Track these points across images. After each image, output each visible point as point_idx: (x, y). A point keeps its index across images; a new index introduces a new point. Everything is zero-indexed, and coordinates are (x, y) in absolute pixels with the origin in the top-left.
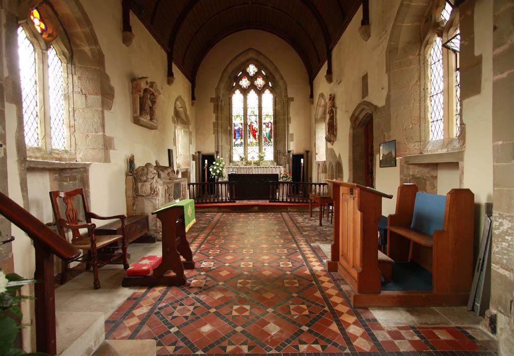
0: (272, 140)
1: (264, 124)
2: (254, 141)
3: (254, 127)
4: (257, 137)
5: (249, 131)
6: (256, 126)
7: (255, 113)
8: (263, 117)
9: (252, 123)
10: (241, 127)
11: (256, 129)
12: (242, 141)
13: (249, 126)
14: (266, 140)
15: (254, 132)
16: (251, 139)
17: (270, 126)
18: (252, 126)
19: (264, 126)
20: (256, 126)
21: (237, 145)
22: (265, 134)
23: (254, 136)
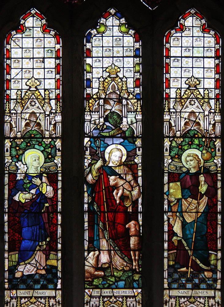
0: (216, 257)
1: (173, 177)
2: (118, 261)
3: (117, 195)
4: (133, 241)
5: (91, 212)
6: (127, 188)
7: (124, 125)
8: (167, 143)
9: (106, 171)
10: (47, 190)
11: (128, 204)
12: (56, 261)
13: (93, 187)
14: (181, 258)
15: (113, 217)
16: (100, 256)
17: (203, 188)
18: (111, 189)
19: (174, 190)
20: (127, 188)
21: (28, 282)
22: (177, 228)
23: (120, 241)
